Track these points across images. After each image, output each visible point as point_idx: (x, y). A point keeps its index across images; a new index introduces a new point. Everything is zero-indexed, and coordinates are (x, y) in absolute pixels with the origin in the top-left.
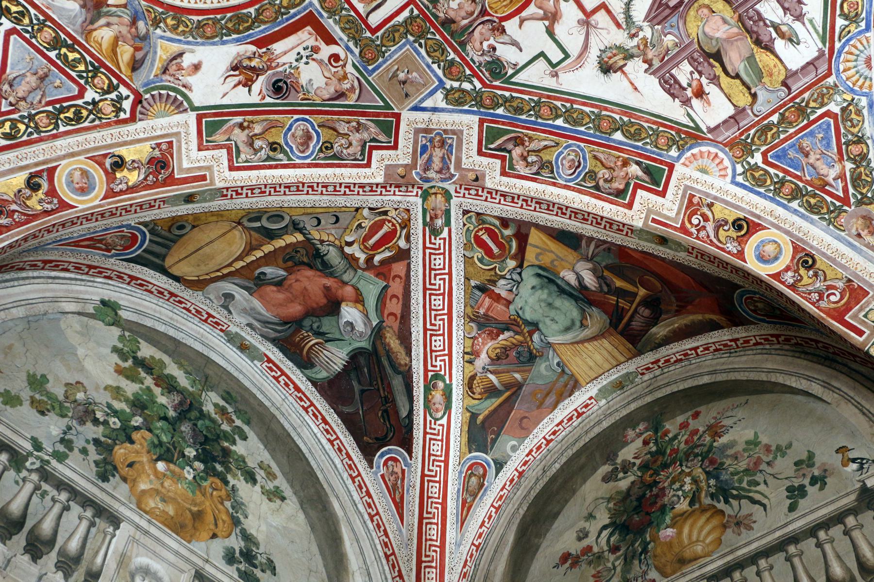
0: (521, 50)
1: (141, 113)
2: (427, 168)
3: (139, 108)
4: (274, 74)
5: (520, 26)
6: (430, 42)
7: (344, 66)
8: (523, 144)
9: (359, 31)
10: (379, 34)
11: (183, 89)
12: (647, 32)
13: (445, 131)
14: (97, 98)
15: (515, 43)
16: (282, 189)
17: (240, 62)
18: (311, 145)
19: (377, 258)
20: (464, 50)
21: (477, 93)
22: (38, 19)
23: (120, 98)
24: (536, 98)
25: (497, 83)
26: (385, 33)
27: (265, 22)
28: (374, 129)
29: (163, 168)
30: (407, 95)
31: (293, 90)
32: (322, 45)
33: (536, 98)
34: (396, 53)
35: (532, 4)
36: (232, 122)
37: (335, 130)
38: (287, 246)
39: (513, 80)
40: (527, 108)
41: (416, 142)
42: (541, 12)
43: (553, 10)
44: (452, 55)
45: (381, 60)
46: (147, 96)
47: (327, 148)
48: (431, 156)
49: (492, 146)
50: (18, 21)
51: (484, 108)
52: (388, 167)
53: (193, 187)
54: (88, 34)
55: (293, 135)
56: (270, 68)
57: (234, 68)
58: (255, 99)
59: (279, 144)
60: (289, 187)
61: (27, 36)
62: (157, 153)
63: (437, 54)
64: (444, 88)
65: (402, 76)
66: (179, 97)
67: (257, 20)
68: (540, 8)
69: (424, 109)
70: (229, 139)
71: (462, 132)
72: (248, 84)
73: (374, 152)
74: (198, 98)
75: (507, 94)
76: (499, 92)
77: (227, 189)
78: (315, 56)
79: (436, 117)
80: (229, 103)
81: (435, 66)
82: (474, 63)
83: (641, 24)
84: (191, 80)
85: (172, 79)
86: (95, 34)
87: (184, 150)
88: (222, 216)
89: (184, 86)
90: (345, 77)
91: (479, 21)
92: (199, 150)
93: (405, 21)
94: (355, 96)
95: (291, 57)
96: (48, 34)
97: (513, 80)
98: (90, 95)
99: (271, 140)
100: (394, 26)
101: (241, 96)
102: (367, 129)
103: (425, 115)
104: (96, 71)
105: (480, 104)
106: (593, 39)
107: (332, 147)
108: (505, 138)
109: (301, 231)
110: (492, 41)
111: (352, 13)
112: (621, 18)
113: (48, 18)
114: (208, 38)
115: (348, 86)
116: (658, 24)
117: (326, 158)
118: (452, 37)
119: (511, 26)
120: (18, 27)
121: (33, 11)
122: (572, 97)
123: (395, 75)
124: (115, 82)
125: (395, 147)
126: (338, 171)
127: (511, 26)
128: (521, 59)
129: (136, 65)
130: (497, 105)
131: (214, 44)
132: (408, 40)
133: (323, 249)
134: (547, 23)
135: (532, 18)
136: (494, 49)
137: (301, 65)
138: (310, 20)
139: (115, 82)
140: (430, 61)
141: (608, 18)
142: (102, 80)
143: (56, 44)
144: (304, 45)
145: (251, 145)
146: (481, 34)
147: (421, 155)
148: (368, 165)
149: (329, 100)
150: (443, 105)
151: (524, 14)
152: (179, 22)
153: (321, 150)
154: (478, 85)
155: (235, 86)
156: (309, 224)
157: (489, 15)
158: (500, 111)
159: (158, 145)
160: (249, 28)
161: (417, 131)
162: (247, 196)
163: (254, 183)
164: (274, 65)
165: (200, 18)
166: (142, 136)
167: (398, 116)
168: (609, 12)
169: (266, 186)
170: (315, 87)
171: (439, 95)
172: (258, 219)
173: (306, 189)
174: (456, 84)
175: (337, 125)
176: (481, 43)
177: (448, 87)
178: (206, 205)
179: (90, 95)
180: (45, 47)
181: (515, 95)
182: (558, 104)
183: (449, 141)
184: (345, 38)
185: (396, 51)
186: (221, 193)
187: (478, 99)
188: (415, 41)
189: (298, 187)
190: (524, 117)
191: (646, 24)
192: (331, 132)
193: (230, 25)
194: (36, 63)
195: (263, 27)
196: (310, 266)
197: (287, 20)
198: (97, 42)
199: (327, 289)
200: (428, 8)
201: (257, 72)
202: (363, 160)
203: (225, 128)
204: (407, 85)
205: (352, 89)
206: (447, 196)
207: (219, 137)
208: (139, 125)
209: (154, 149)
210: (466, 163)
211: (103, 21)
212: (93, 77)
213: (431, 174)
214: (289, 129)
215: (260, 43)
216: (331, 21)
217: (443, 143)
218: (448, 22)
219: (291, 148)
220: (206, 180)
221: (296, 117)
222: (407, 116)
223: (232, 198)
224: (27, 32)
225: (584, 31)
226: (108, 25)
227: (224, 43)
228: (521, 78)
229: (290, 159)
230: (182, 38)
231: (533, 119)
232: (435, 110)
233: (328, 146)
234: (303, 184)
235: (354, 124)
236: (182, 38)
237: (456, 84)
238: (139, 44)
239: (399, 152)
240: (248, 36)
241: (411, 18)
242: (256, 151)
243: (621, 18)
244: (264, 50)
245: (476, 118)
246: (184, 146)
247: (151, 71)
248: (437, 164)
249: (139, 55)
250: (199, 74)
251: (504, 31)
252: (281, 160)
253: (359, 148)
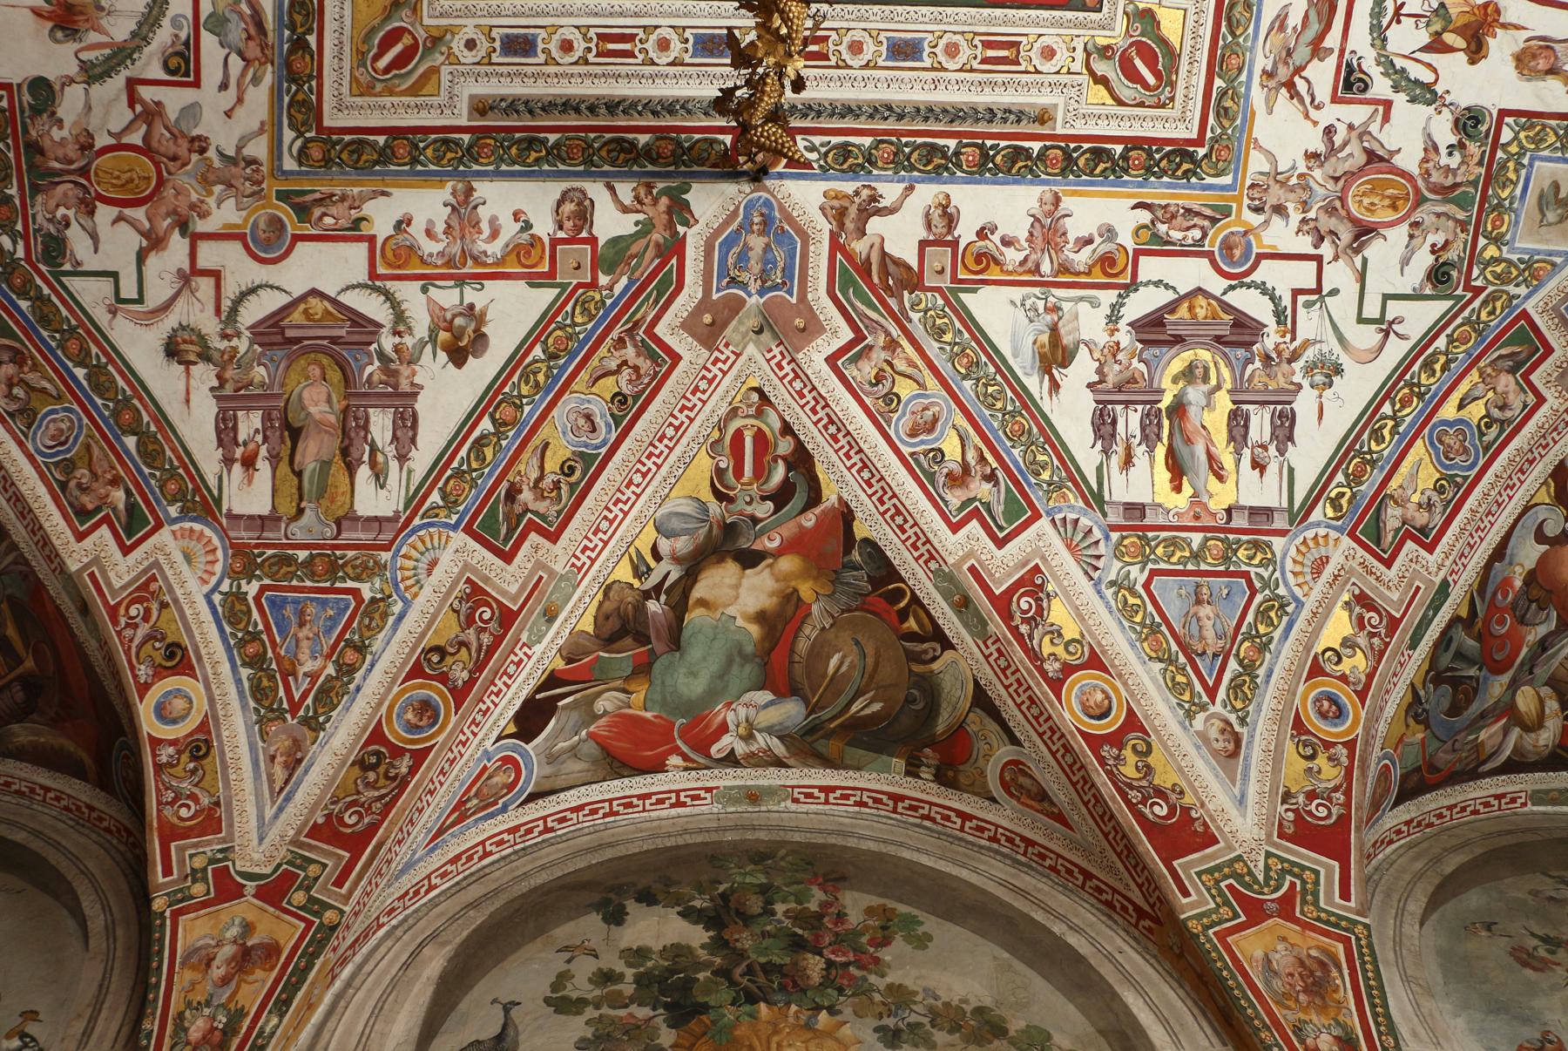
0: (96, 251)
5: (114, 222)
8: (21, 367)
12: (242, 345)
15: (94, 237)
20: (32, 197)
21: (13, 260)
24: (73, 322)
25: (43, 268)
33: (73, 322)
35: (144, 208)
39: (64, 279)
40: (55, 325)
42: (147, 225)
43: (161, 233)
44: (13, 191)
68: (149, 220)
75: (46, 291)
76: (39, 282)
83: (243, 329)
97: (64, 279)
106: (180, 304)
108: (7, 342)
110: (71, 213)
112: (226, 304)
116: (260, 345)
118: (29, 170)
119: (104, 213)
122: (115, 355)
127: (104, 213)
128: (91, 262)
130: (23, 294)
134: (145, 243)
135: (133, 224)
136: (68, 225)
141: (212, 293)
146: (65, 194)
151: (127, 212)
154: (20, 253)
157: (89, 180)
158: (24, 305)
168: (218, 287)
176: (58, 206)
181: (54, 298)
182: (94, 350)
190: (45, 334)
191: (247, 333)
225: (177, 286)
228: (75, 284)
231: (53, 344)
243: (226, 304)
251: (91, 212)
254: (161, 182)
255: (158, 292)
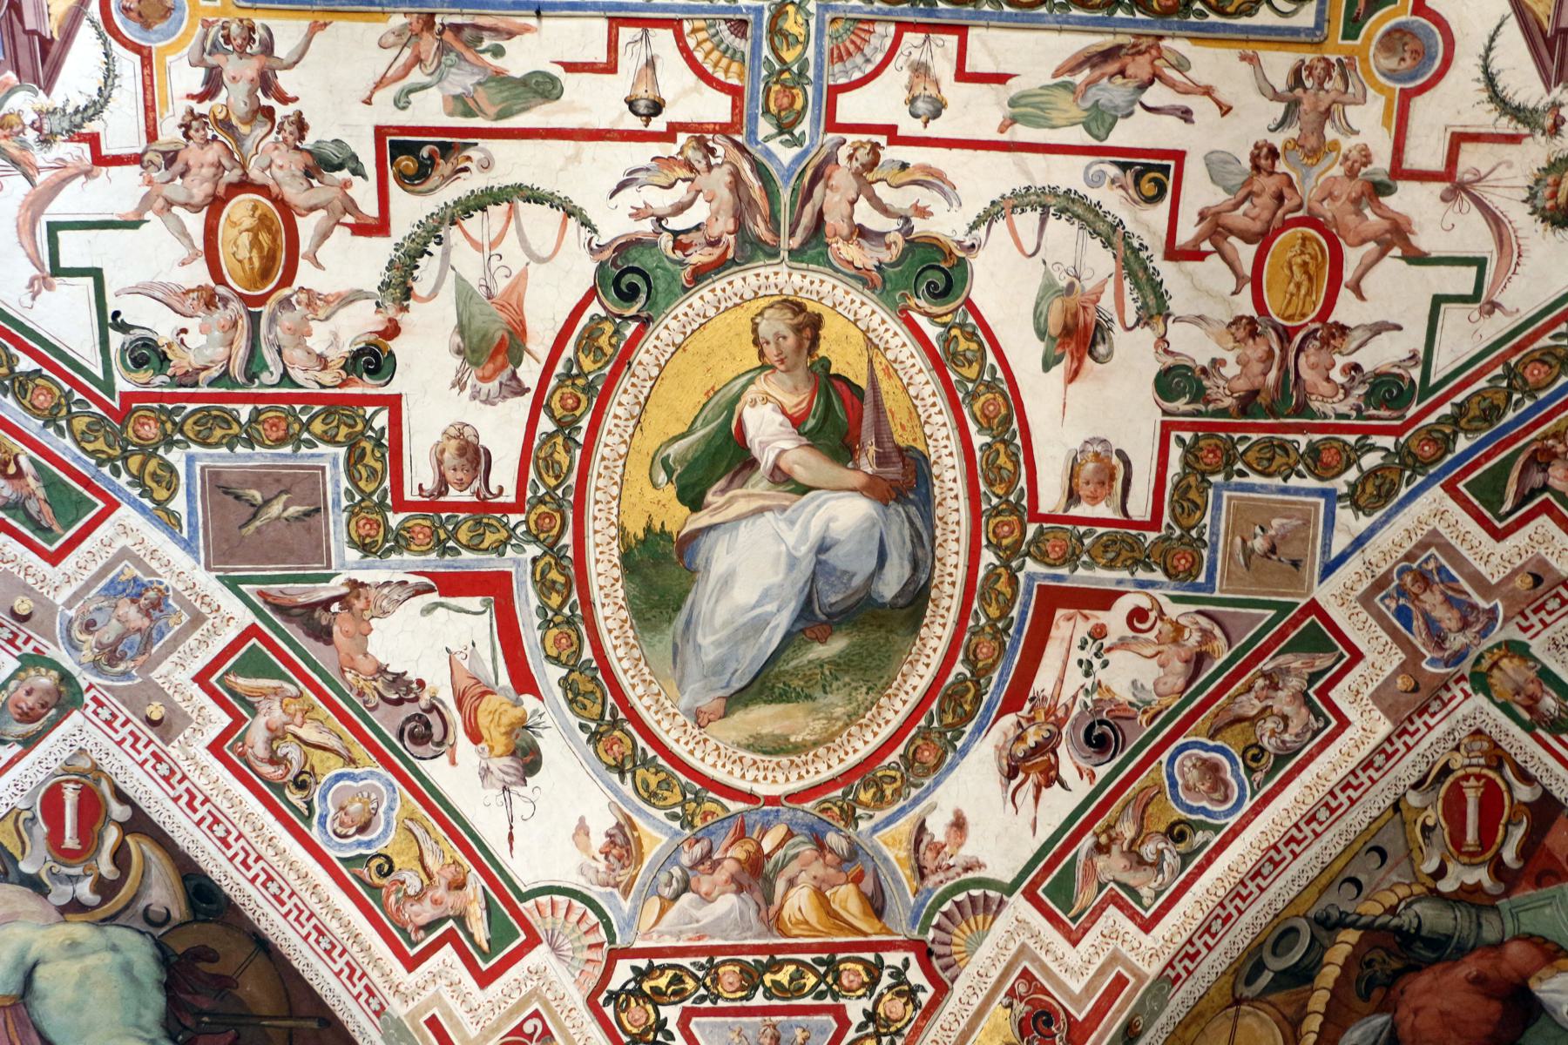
0: (1399, 328)
1: (946, 968)
2: (1437, 637)
3: (936, 963)
4: (1074, 727)
5: (1361, 297)
6: (1251, 456)
7: (1161, 613)
8: (1555, 456)
9: (1134, 544)
10: (1166, 519)
11: (970, 875)
13: (1409, 557)
14: (868, 1004)
15: (1379, 328)
16: (1252, 886)
17: (1011, 756)
18: (1229, 777)
19: (1509, 855)
20: (1313, 415)
21: (1397, 453)
22: (702, 967)
23: (899, 974)
24: (1499, 371)
25: (1413, 410)
26: (1173, 510)
27: (993, 666)
28: (1296, 662)
29: (1049, 1023)
30: (1296, 564)
31: (1123, 724)
32: (1101, 617)
33: (1499, 371)
34: (1216, 522)
35: (1347, 250)
36: (1082, 857)
37: (1240, 720)
38: (1345, 968)
39: (1433, 380)
40: (1500, 399)
41: (1381, 618)
42: (1371, 246)
43: (1386, 224)
44: (1303, 441)
45: (1205, 553)
46: (931, 934)
47: (1255, 758)
48: (1426, 616)
49: (1507, 506)
50: (681, 995)
51: (1432, 463)
52: (1376, 697)
53: (1120, 1011)
54: (775, 923)
55: (1187, 788)
56: (1059, 724)
57: (1011, 773)
58: (1082, 789)
59: (1180, 822)
60: (1258, 873)
61: (708, 1004)
62: (1021, 1008)
63: (1279, 461)
64: (1340, 498)
65: (1259, 544)
66: (975, 892)
67: (979, 674)
68: (1363, 242)
69: (1343, 558)
70: (1101, 886)
71: (1435, 532)
72: (1051, 776)
73: (1333, 694)
74: (1002, 868)
75: (1446, 409)
76: (1431, 419)
77: (1170, 965)
78: (1107, 643)
79: (1371, 551)
80: (1051, 831)
81: (1294, 481)
82: (1348, 417)
84: (968, 851)
85: (941, 876)
86: (785, 914)
87: (1053, 967)
88: (1201, 1015)
89: (967, 869)
90: (1178, 629)
91: (1292, 354)
92: (1075, 943)
93: (1186, 463)
94: (1221, 641)
95: (1075, 678)
96: (730, 975)
97: (1433, 380)
98: (855, 1010)
99: (1163, 828)
100: (1176, 487)
101: (1059, 805)
102: (1288, 671)
103: (1354, 564)
104: (831, 964)
105: (1420, 465)
106: (1494, 200)
107: (1263, 750)
108: (1515, 474)
109: (1342, 923)
110: (1341, 361)
111: (1100, 530)
112: (1506, 125)
113: (711, 951)
114: (936, 767)
115: (1196, 636)
117: (1269, 775)
118: (1276, 416)
119: (1347, 310)
120: (688, 1003)
121: (685, 962)
123: (1248, 553)
124: (870, 956)
125: (1357, 656)
126: (1306, 776)
127: (1347, 310)
128: (1414, 338)
129: (876, 905)
130: (1447, 442)
131: (951, 767)
132: (1217, 486)
133: (1406, 920)
134: (1397, 251)
135: (1366, 268)
136: (1357, 367)
137: (1100, 674)
138: (1052, 599)
139: (870, 956)
140: (1278, 481)
141: (1484, 147)
142: (853, 973)
143: (751, 979)
144: (1077, 642)
145: (1141, 862)
146: (1313, 367)
147: (1409, 627)
148: (1344, 723)
149: (1188, 684)
150: (1364, 522)
151: (1348, 275)
152: (878, 784)
153: (1250, 771)
154: (1388, 442)
155: (1037, 798)
156: (1343, 901)
157: (1297, 329)
158: (1463, 444)
159: (1011, 993)
160: (978, 698)
161: (1366, 600)
162: (1210, 948)
163: (1200, 917)
164: (1060, 713)
165: (900, 749)
166: (976, 1002)
167: (1314, 607)
168: (1476, 138)
169: (1221, 905)
170: (1149, 686)
171: (1344, 515)
172: (1259, 967)
173: (1286, 852)
174: (1352, 474)
175: (1238, 710)
176: (1328, 379)
177: (1344, 490)
178: (1163, 1019)
179: (855, 1010)
180: (741, 999)
181: (1459, 398)
182: (1545, 341)
183: (1431, 565)
184: (1125, 574)
185: (1215, 520)
186: (1168, 980)
187: (1410, 461)
188: (1228, 477)
189: (1272, 860)
190: (1510, 415)
192: (1238, 728)
193: (949, 719)
194: (749, 1033)
195: (995, 676)
196: (1416, 968)
197: (1019, 631)
198: (798, 923)
199: (1478, 981)
200: (1198, 413)
201: (1047, 746)
202: (1328, 723)
203: (1079, 874)
204: (1281, 550)
205: (1207, 635)
206: (1518, 650)
207: (1086, 897)
208: (959, 988)
209: (1010, 1006)
210: (1493, 573)
211: (780, 885)
212: (837, 979)
213: (1456, 641)
214: (1173, 784)
215: (1012, 703)
216: (1081, 572)
217: (1424, 578)
218: (1248, 402)
219: (1203, 810)
220: (1127, 982)
221: (1165, 757)
222: (1326, 593)
223: (1189, 973)
224: (703, 998)
225: (1467, 202)
226: (791, 883)
227: (964, 752)
228: (1443, 364)
229: (1217, 829)
230: (902, 803)
231: (1528, 403)
232: (1359, 542)
233: (1253, 754)
234: (1275, 847)
235: (1260, 682)
236: (902, 803)
237: (1352, 474)
238: (853, 870)
239: (1370, 657)
240: (988, 708)
241: (1190, 451)
242: (1157, 866)
243: (1506, 125)
244: (1028, 706)
245: (1437, 491)
246: (1047, 960)
247: (904, 894)
248: (1447, 618)
249: (868, 885)
250: (972, 831)
251: (1343, 330)
252: (1206, 843)
253: (1304, 711)
254: (1312, 221)
255: (1473, 235)
